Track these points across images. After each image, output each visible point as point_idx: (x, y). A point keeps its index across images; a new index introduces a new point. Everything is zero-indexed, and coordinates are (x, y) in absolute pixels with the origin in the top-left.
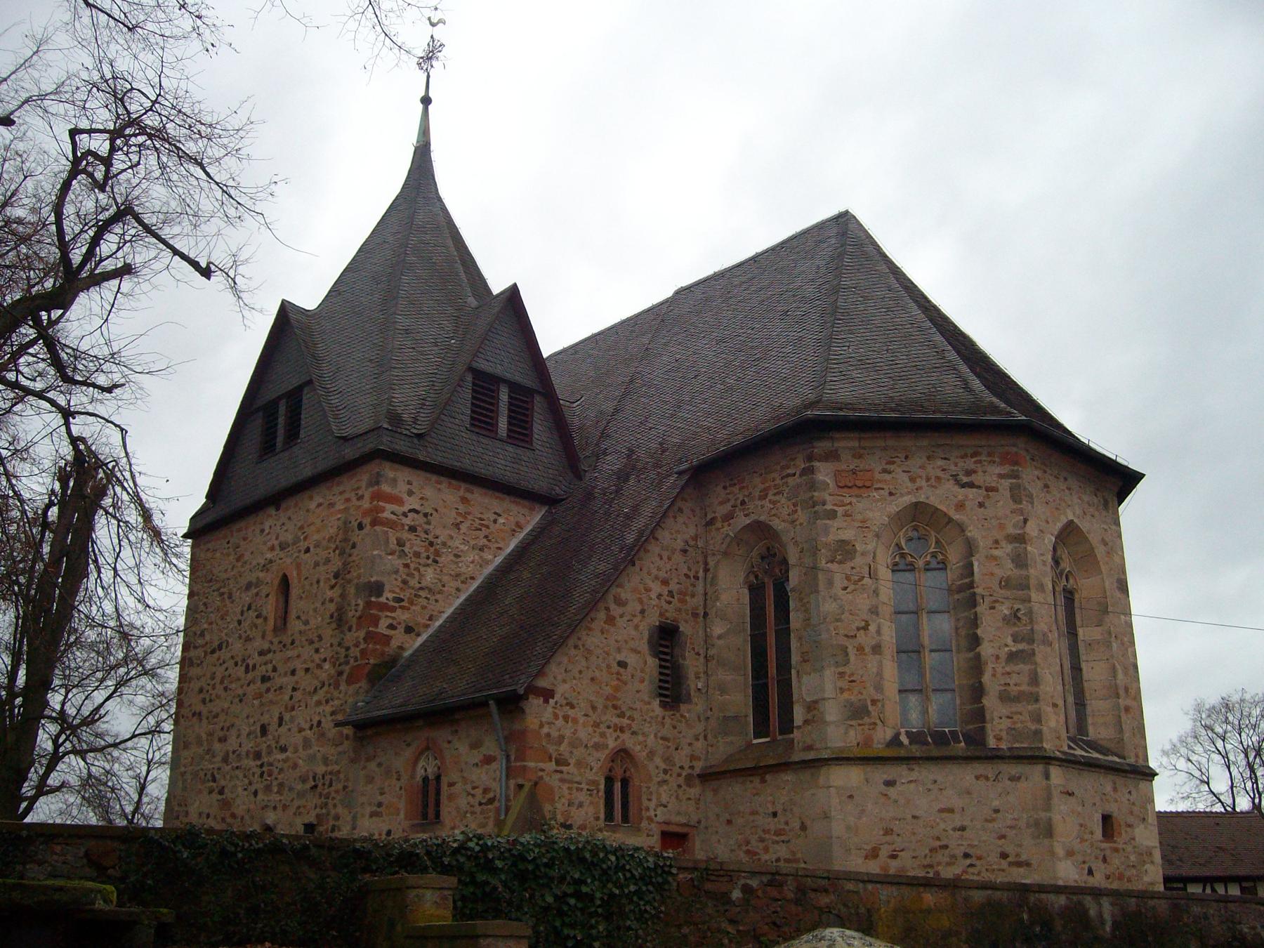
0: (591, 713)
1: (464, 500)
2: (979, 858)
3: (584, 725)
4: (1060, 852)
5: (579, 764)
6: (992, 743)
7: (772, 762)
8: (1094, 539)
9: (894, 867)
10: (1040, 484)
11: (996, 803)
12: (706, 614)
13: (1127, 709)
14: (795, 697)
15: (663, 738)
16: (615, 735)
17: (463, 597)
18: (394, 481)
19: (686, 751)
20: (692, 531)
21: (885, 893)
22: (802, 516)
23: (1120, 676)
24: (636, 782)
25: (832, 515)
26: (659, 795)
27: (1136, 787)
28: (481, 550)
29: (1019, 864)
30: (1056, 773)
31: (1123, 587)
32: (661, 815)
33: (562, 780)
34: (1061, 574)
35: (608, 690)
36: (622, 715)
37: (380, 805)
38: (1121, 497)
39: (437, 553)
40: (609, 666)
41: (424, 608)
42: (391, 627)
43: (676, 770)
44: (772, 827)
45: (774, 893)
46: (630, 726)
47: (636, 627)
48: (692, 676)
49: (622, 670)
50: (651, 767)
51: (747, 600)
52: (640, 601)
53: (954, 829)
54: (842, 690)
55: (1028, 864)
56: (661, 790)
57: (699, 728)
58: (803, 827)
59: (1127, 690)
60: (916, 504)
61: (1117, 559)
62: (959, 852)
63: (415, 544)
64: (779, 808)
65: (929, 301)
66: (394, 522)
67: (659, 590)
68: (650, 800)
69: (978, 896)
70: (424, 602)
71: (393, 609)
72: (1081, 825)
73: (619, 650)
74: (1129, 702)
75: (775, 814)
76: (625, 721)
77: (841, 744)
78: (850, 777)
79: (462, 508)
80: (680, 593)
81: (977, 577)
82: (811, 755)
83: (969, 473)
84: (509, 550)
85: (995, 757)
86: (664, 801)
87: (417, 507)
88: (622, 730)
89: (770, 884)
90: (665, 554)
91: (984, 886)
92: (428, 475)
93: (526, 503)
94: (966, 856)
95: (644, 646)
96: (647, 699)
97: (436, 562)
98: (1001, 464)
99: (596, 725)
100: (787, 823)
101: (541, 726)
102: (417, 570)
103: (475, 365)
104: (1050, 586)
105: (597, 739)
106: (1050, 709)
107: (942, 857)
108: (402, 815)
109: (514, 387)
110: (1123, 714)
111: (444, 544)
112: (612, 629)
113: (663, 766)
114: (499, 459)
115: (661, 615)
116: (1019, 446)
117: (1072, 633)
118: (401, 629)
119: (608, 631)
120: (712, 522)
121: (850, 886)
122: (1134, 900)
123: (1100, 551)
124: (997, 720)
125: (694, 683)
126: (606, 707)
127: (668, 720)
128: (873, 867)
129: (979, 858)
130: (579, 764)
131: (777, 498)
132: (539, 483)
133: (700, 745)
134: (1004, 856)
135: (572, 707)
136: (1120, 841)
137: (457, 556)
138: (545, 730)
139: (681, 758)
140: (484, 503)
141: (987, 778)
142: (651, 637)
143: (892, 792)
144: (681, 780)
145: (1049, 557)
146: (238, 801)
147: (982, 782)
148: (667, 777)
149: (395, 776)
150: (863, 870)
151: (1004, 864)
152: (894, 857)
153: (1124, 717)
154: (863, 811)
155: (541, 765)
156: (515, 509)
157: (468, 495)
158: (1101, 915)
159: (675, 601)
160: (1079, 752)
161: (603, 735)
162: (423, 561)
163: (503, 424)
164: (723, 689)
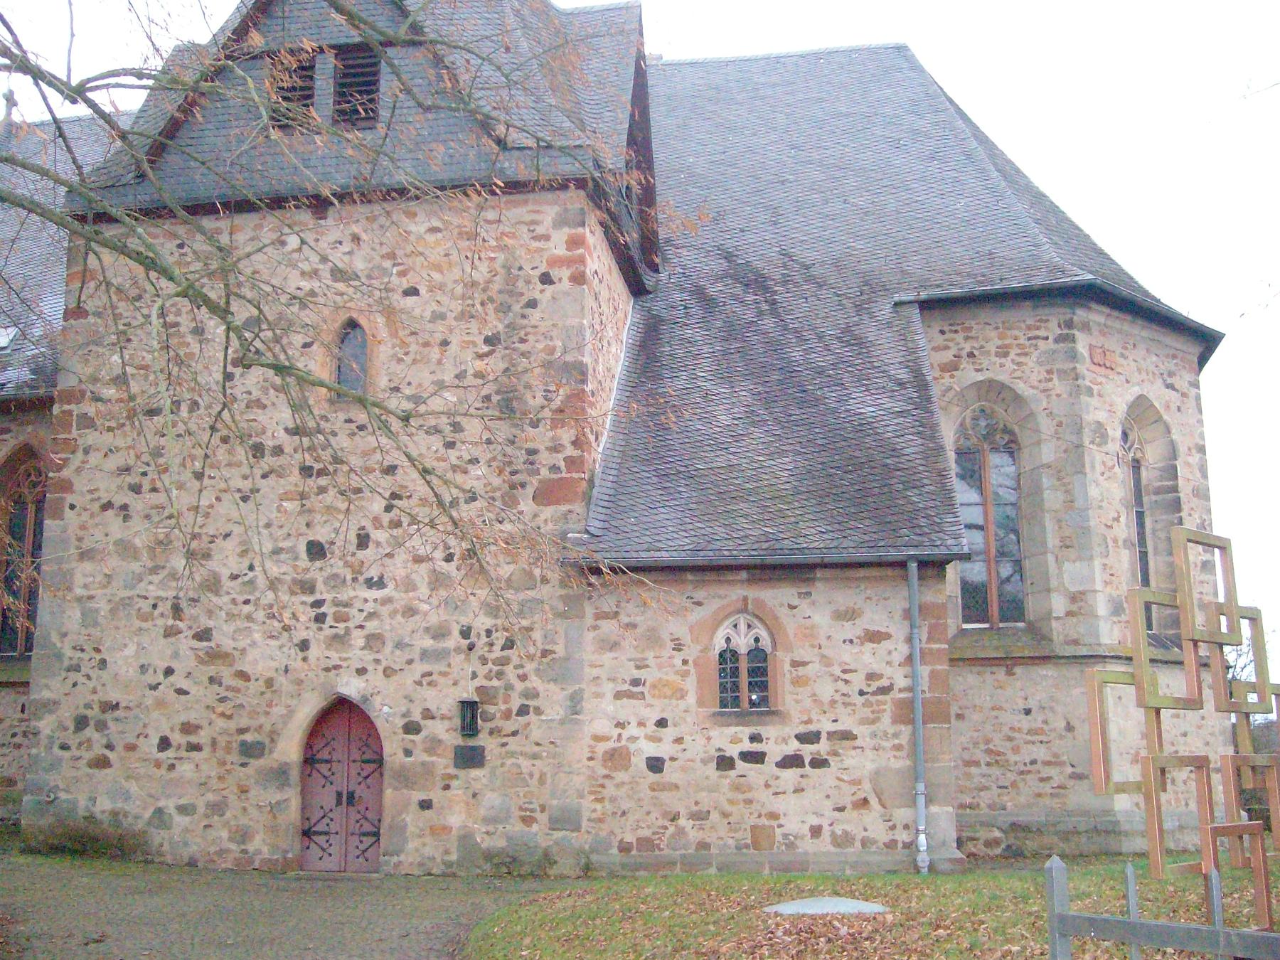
22: (1057, 385)
25: (1090, 392)
37: (636, 682)
58: (1069, 728)
64: (1032, 703)
75: (1028, 712)
81: (1180, 482)
83: (1171, 374)
100: (1045, 722)
108: (691, 699)
131: (1022, 359)
146: (252, 654)
149: (671, 645)
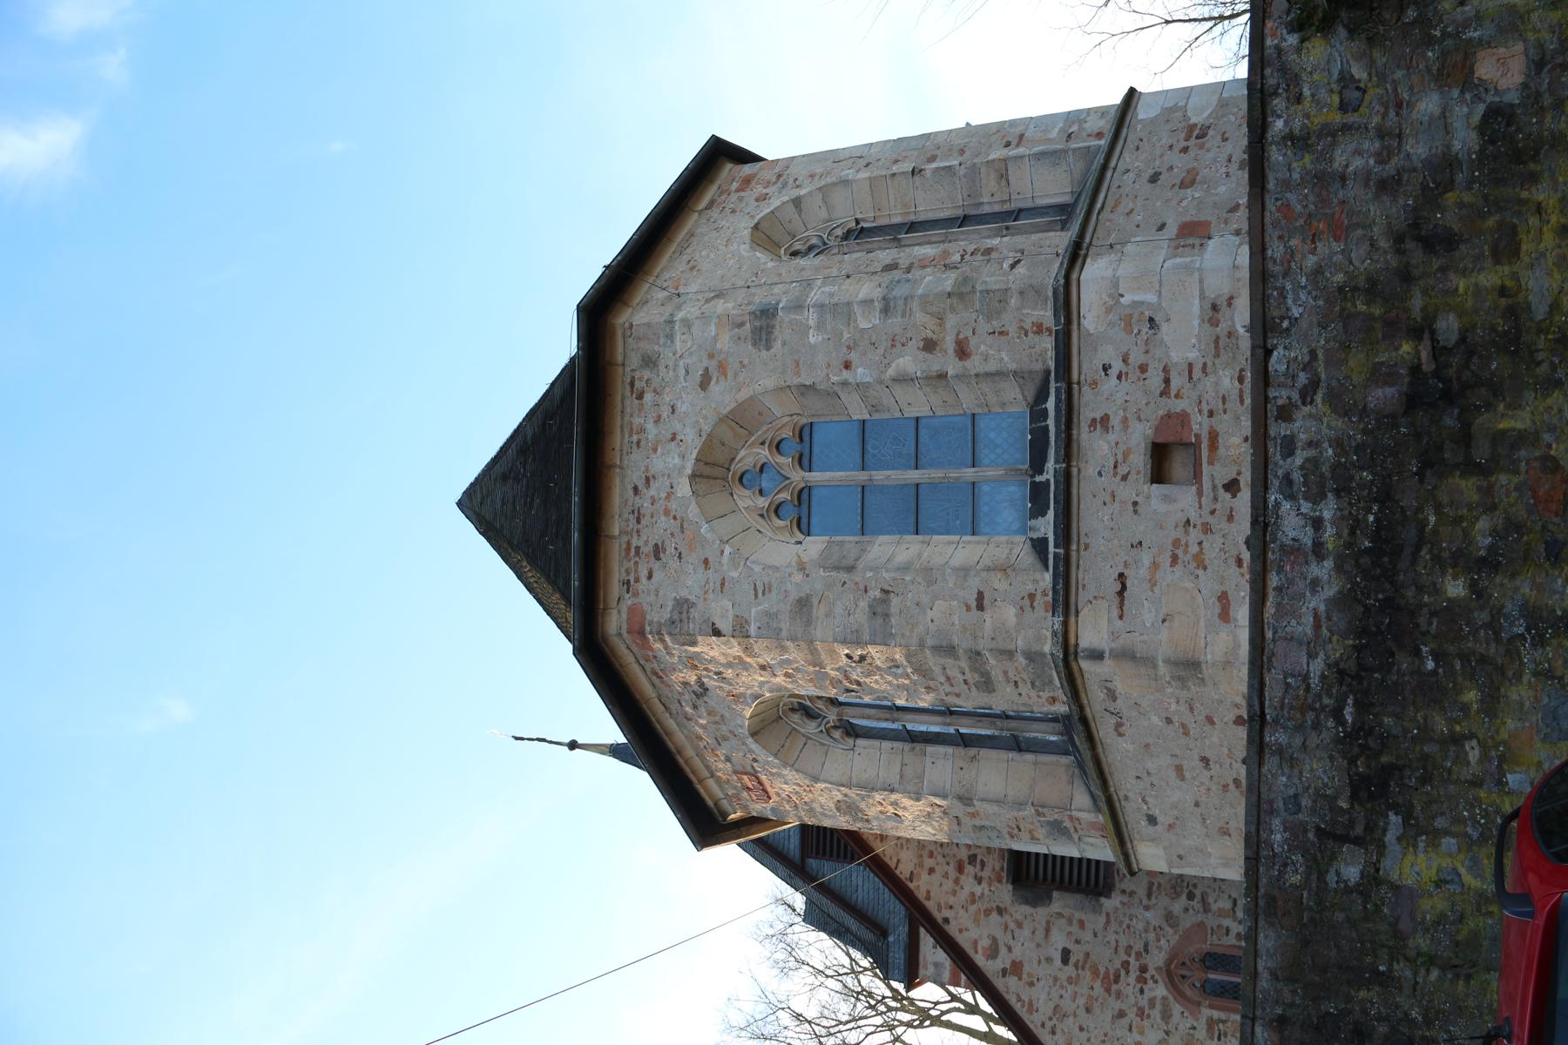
0: (1125, 1021)
15: (1149, 896)
16: (1150, 982)
26: (1222, 913)
36: (1126, 965)
40: (1070, 980)
46: (1139, 955)
49: (1073, 960)
50: (1187, 921)
52: (988, 912)
56: (1214, 907)
67: (971, 880)
68: (1228, 930)
72: (1175, 559)
73: (1049, 960)
76: (1132, 960)
86: (1228, 905)
88: (1143, 969)
90: (929, 863)
95: (1041, 913)
96: (1103, 919)
99: (1141, 1013)
105: (1156, 1013)
112: (1026, 969)
119: (1029, 975)
122: (1258, 1030)
124: (1024, 699)
126: (1119, 995)
142: (1027, 902)
148: (1198, 893)
153: (974, 364)
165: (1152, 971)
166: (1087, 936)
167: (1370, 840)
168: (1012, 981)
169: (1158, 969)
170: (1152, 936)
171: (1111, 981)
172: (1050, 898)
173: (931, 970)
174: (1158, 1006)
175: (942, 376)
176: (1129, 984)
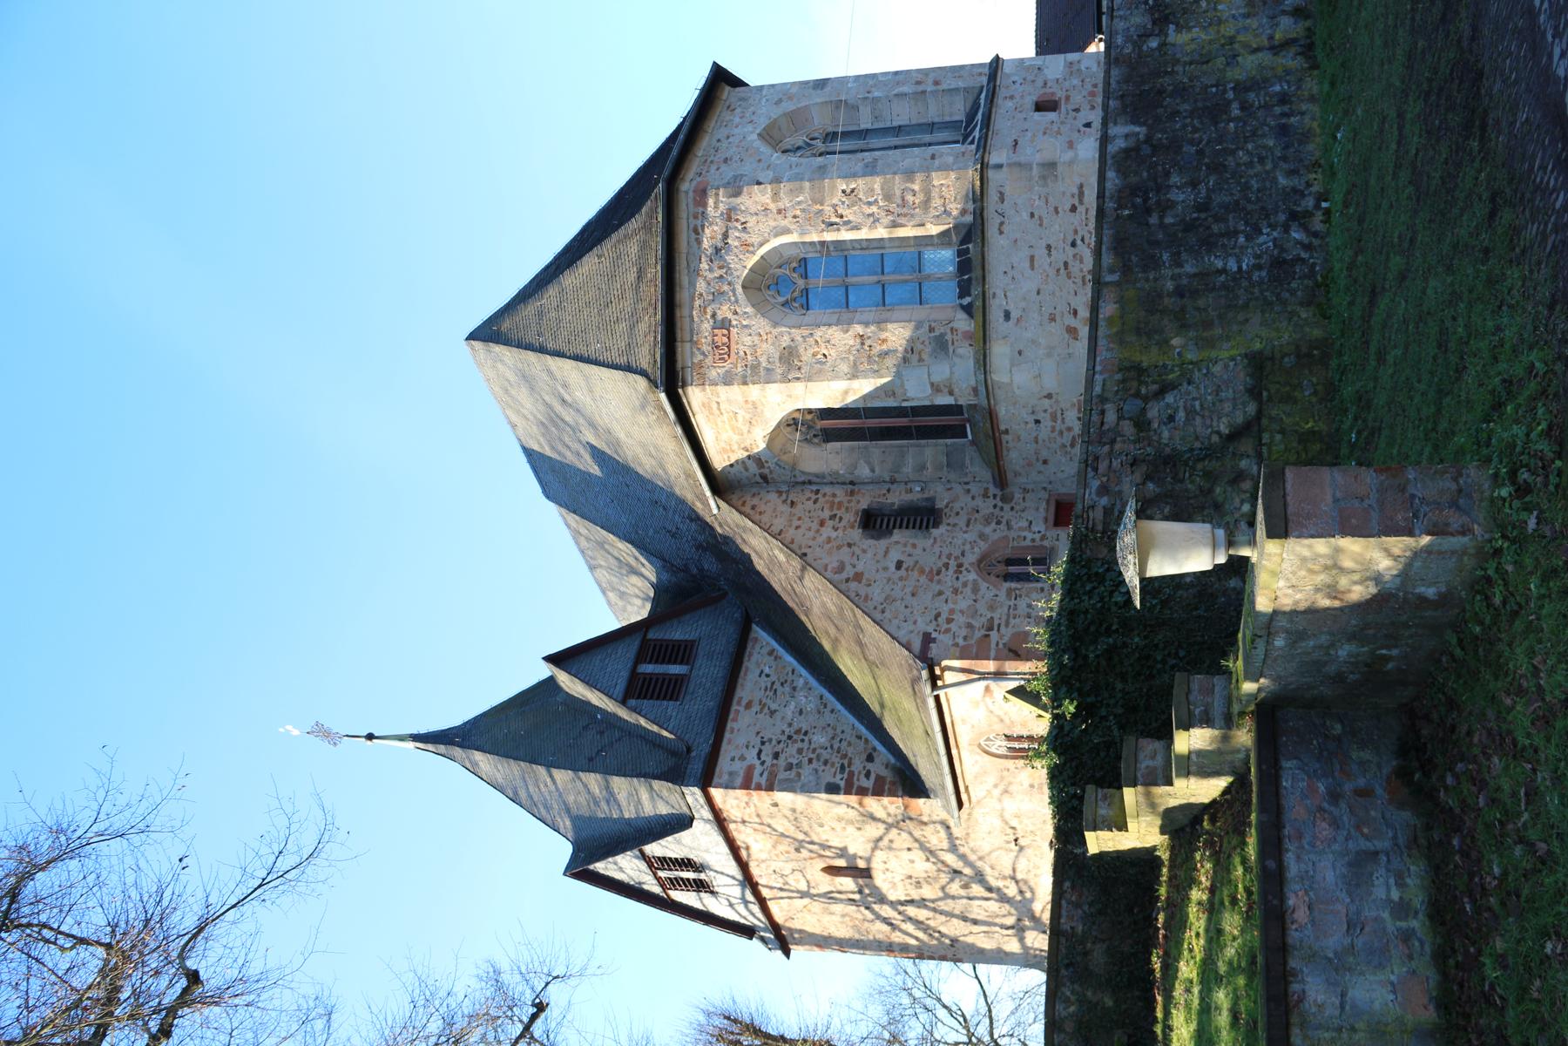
1: (749, 706)
2: (1076, 232)
3: (955, 603)
4: (1069, 155)
5: (992, 608)
6: (969, 218)
7: (988, 425)
8: (776, 112)
9: (1084, 313)
10: (724, 167)
11: (1025, 215)
12: (852, 483)
13: (936, 83)
14: (927, 403)
17: (839, 707)
18: (731, 774)
19: (979, 502)
20: (773, 496)
21: (1103, 354)
23: (905, 89)
24: (1008, 553)
26: (1021, 529)
27: (1009, 76)
28: (794, 689)
29: (1081, 194)
30: (994, 159)
31: (821, 84)
32: (1039, 526)
33: (1007, 625)
34: (809, 145)
35: (923, 579)
36: (946, 566)
38: (736, 82)
39: (798, 732)
40: (901, 579)
41: (849, 744)
42: (868, 775)
43: (997, 511)
44: (1050, 424)
45: (1103, 466)
47: (864, 551)
48: (908, 497)
50: (996, 536)
51: (838, 444)
52: (839, 548)
53: (1050, 255)
54: (921, 360)
55: (1081, 186)
57: (958, 489)
58: (1049, 396)
59: (918, 83)
60: (744, 287)
61: (794, 90)
62: (1070, 251)
63: (790, 753)
64: (1031, 419)
65: (551, 264)
66: (770, 773)
69: (1108, 259)
70: (844, 744)
71: (851, 774)
73: (886, 569)
74: (930, 81)
75: (1037, 422)
77: (971, 363)
78: (1000, 352)
79: (756, 708)
80: (831, 508)
82: (982, 389)
84: (795, 663)
85: (980, 215)
86: (1026, 524)
87: (755, 751)
88: (960, 566)
89: (1096, 470)
91: (1097, 253)
92: (725, 741)
93: (750, 645)
94: (1073, 244)
95: (883, 543)
97: (806, 733)
98: (705, 205)
99: (956, 591)
101: (956, 645)
102: (814, 750)
103: (620, 697)
104: (820, 159)
105: (968, 590)
106: (937, 162)
107: (1075, 268)
109: (640, 658)
110: (940, 88)
111: (790, 725)
112: (866, 576)
113: (993, 525)
114: (706, 672)
115: (852, 527)
116: (686, 187)
117: (863, 134)
118: (869, 766)
120: (764, 477)
121: (1098, 389)
123: (789, 106)
125: (916, 495)
126: (939, 582)
127: (951, 521)
128: (1084, 331)
129: (1076, 232)
130: (992, 608)
132: (732, 631)
133: (974, 488)
134: (1074, 209)
135: (938, 616)
136: (1060, 94)
137: (801, 712)
138: (961, 641)
139: (986, 507)
140: (750, 687)
141: (1002, 224)
142: (873, 537)
143: (1014, 315)
144: (1007, 507)
145: (793, 159)
147: (1005, 228)
150: (1086, 342)
151: (1081, 209)
152: (1075, 313)
153: (944, 86)
154: (1033, 342)
155: (993, 645)
156: (755, 657)
157: (744, 703)
158: (1127, 136)
159: (839, 513)
160: (977, 133)
161: (965, 585)
162: (805, 745)
163: (675, 669)
164: (923, 467)
165: (966, 565)
166: (918, 551)
167: (1163, 33)
168: (853, 585)
169: (972, 564)
170: (968, 547)
171: (934, 574)
172: (891, 533)
173: (726, 777)
174: (970, 586)
175: (924, 92)
176: (948, 577)
